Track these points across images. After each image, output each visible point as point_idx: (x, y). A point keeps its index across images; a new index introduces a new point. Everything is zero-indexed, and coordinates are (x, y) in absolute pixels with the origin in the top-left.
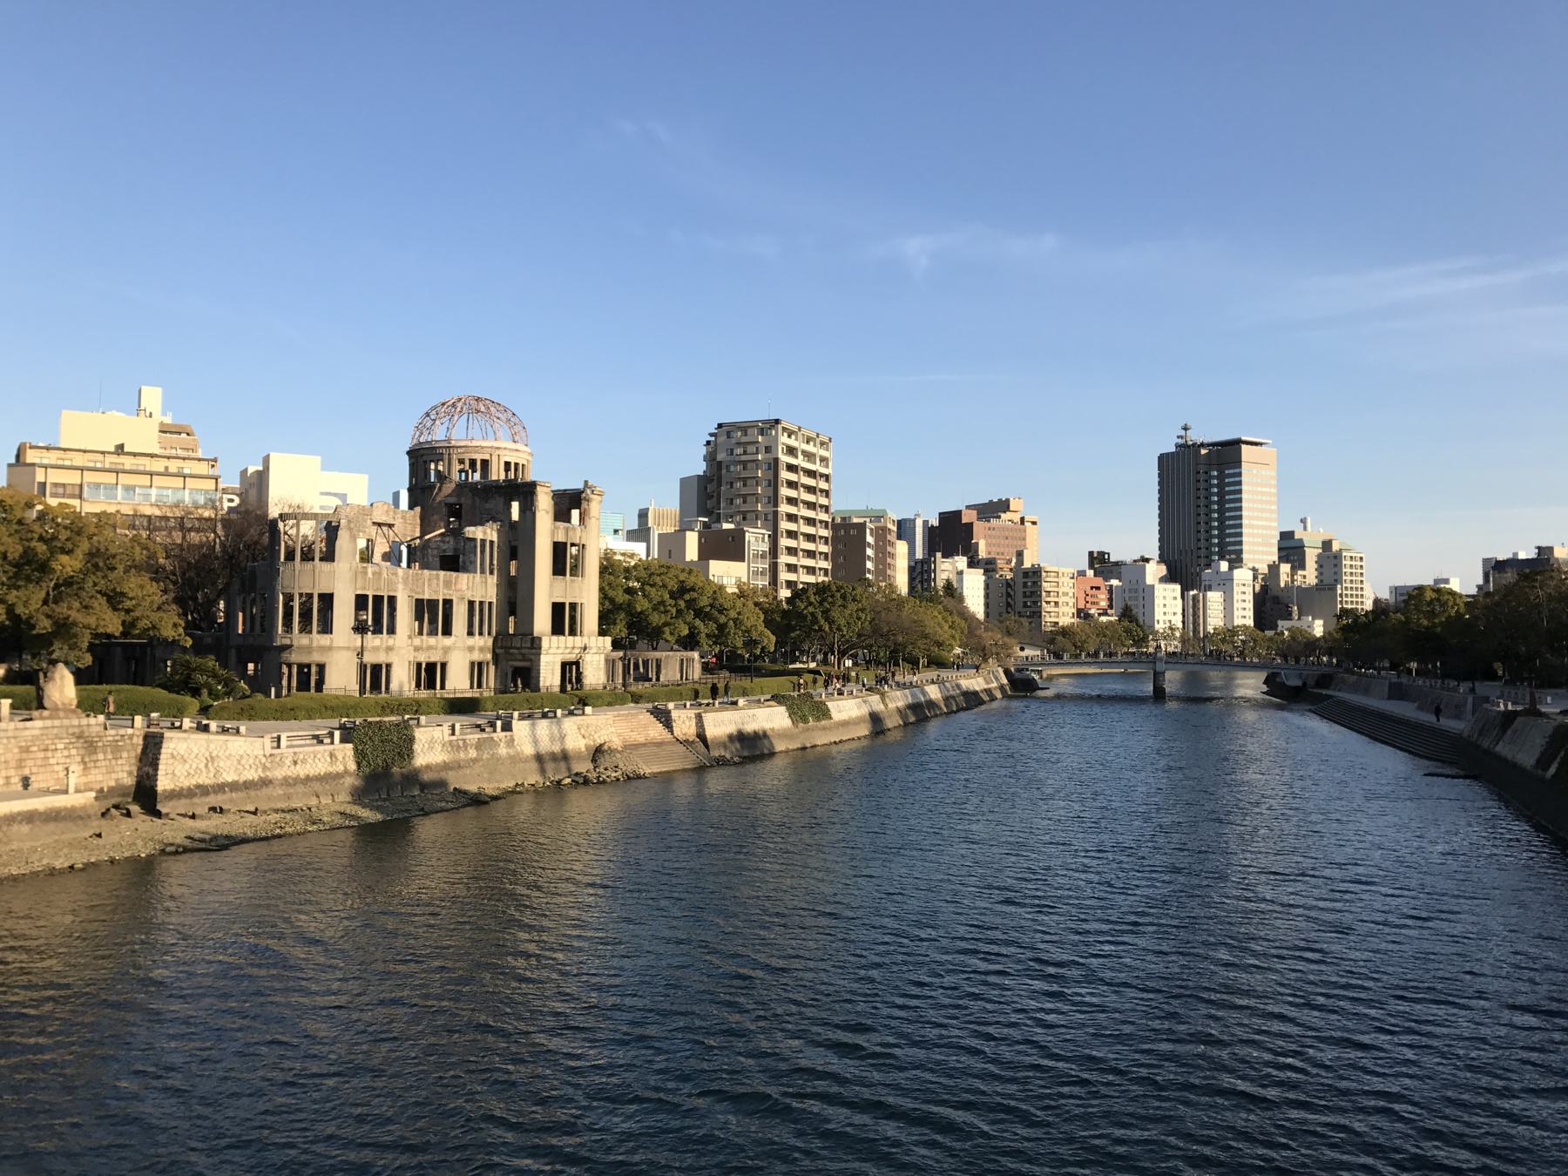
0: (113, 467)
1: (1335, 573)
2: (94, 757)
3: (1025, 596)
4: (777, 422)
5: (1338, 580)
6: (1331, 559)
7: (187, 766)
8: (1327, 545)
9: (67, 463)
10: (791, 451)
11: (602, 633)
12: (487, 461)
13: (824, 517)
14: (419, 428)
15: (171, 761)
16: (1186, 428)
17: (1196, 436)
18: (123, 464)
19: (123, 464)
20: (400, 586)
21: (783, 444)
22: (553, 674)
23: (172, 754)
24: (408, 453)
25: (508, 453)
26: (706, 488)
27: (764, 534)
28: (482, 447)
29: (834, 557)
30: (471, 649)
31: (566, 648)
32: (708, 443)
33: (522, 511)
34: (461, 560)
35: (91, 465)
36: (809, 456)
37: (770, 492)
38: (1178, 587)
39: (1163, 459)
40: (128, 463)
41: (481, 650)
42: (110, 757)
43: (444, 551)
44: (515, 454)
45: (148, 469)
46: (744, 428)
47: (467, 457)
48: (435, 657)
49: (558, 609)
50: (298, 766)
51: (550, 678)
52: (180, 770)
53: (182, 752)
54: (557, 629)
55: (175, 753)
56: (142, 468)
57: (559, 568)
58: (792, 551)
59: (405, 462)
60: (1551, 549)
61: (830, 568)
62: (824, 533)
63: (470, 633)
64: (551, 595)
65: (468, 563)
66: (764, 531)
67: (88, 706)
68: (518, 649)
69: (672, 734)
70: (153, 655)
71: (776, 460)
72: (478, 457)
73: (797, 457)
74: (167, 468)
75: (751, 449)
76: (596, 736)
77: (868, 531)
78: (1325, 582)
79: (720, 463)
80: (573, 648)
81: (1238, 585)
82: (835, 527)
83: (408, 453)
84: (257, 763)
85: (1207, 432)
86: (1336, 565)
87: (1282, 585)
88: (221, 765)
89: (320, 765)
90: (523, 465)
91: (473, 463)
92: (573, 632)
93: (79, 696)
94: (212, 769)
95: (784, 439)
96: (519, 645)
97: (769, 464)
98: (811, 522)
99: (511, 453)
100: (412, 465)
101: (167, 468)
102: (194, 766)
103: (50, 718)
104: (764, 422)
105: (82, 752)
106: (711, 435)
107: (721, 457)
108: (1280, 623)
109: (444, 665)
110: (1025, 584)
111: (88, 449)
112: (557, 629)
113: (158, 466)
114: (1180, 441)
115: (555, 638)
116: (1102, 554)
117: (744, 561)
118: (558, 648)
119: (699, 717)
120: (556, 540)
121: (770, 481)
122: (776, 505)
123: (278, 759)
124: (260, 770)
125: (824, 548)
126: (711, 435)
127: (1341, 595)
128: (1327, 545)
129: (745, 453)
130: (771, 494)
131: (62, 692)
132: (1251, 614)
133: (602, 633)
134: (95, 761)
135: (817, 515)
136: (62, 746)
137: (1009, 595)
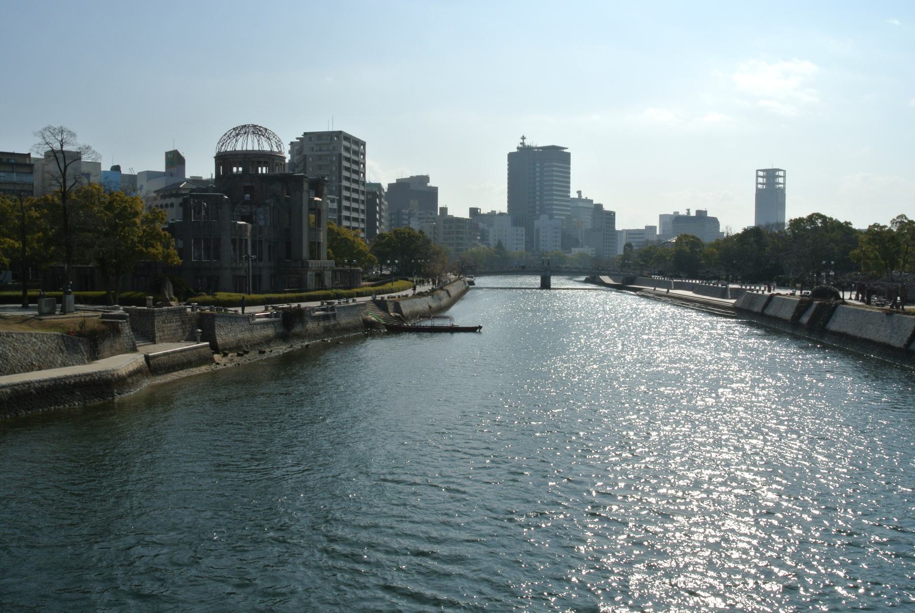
3: (444, 234)
10: (347, 149)
11: (329, 258)
13: (362, 188)
14: (222, 142)
16: (523, 138)
17: (528, 143)
36: (356, 153)
38: (524, 229)
39: (511, 156)
46: (320, 135)
62: (362, 198)
63: (270, 260)
66: (334, 197)
71: (340, 155)
72: (262, 160)
79: (305, 156)
82: (368, 193)
85: (538, 140)
98: (356, 191)
106: (297, 139)
107: (306, 152)
108: (573, 249)
110: (445, 228)
114: (520, 146)
116: (477, 209)
122: (340, 181)
129: (320, 150)
132: (559, 244)
137: (435, 232)
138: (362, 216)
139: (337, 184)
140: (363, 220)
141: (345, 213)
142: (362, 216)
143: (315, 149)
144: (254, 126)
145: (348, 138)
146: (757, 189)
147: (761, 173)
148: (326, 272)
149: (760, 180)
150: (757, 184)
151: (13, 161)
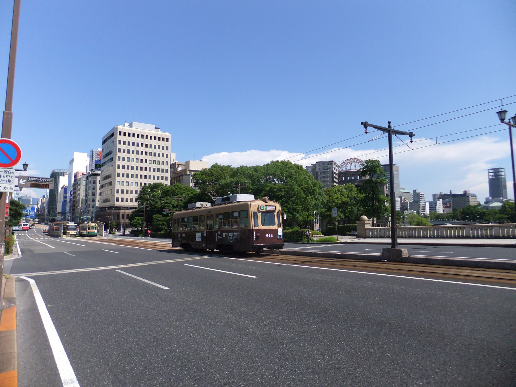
1: (418, 198)
5: (418, 201)
6: (416, 195)
8: (415, 191)
60: (466, 191)
78: (415, 201)
81: (397, 202)
86: (418, 196)
87: (403, 202)
95: (334, 166)
104: (329, 161)
106: (312, 165)
127: (420, 204)
128: (415, 191)
129: (324, 169)
130: (332, 180)
146: (490, 179)
147: (491, 171)
149: (491, 174)
150: (489, 176)
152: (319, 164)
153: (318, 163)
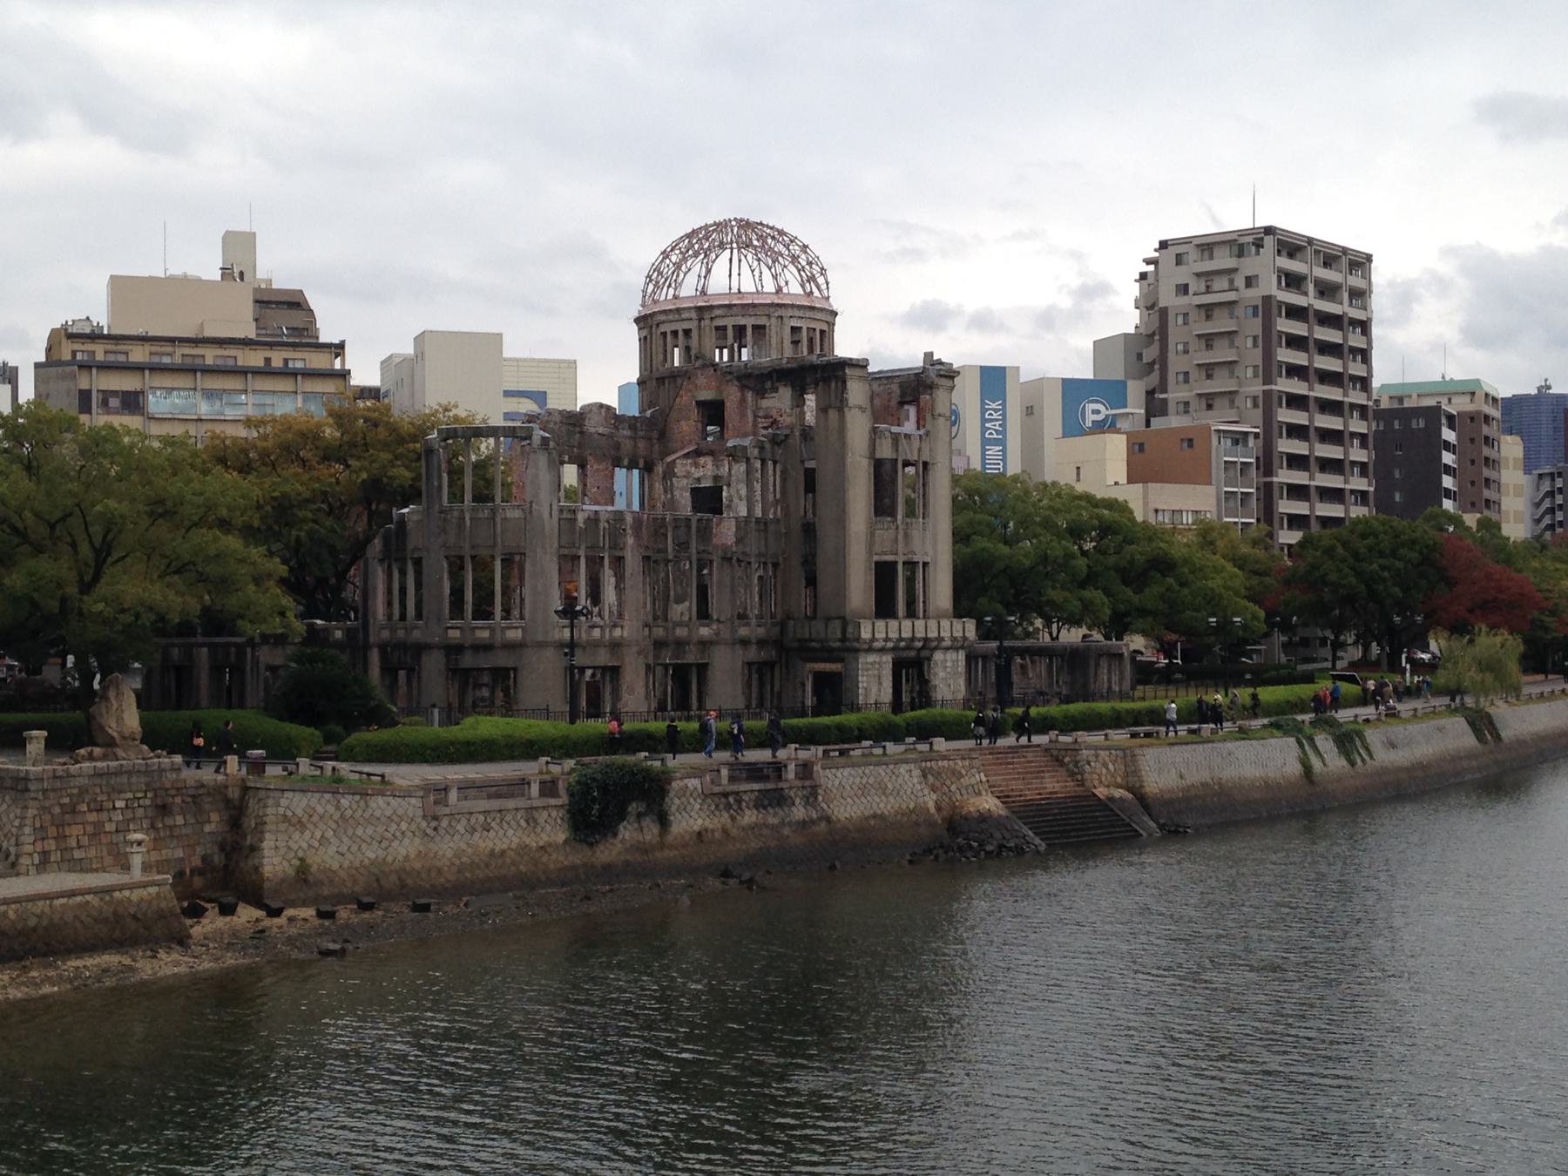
0: (188, 361)
2: (168, 821)
4: (1269, 230)
7: (307, 834)
9: (122, 358)
10: (1293, 281)
11: (959, 612)
12: (763, 327)
13: (1356, 397)
14: (656, 277)
15: (283, 827)
18: (203, 356)
19: (203, 356)
20: (630, 541)
21: (1280, 270)
22: (880, 684)
23: (285, 816)
24: (637, 321)
25: (797, 313)
26: (1140, 356)
27: (1246, 434)
28: (754, 306)
29: (1379, 470)
30: (745, 642)
31: (901, 639)
32: (1143, 276)
33: (823, 410)
34: (724, 494)
35: (156, 359)
36: (1327, 290)
37: (1256, 356)
40: (210, 356)
41: (761, 643)
42: (193, 821)
43: (698, 480)
44: (808, 314)
45: (240, 363)
46: (1207, 246)
47: (729, 322)
48: (691, 657)
49: (884, 574)
50: (477, 835)
51: (874, 690)
52: (300, 841)
53: (299, 812)
54: (884, 609)
55: (289, 814)
56: (231, 362)
57: (883, 504)
58: (1296, 462)
59: (632, 335)
61: (1372, 489)
62: (1358, 426)
64: (870, 553)
65: (736, 500)
67: (153, 738)
68: (821, 641)
69: (1082, 783)
70: (256, 661)
71: (1267, 300)
72: (749, 322)
73: (1306, 294)
74: (268, 360)
75: (1221, 283)
76: (953, 788)
77: (1444, 421)
79: (1164, 312)
80: (913, 639)
82: (1381, 415)
83: (637, 321)
84: (413, 827)
88: (359, 832)
89: (510, 833)
90: (822, 332)
91: (740, 331)
92: (911, 614)
93: (143, 723)
94: (345, 839)
96: (822, 636)
97: (1255, 308)
99: (801, 314)
100: (644, 341)
101: (268, 360)
102: (318, 834)
103: (104, 757)
105: (150, 813)
106: (1148, 262)
107: (1168, 298)
109: (703, 668)
111: (154, 332)
112: (884, 609)
113: (255, 359)
115: (880, 624)
117: (1210, 484)
118: (887, 639)
119: (1129, 758)
120: (878, 456)
121: (1255, 338)
123: (445, 823)
124: (417, 841)
125: (1359, 454)
126: (1148, 262)
129: (1208, 290)
131: (120, 720)
133: (959, 612)
134: (171, 828)
135: (1346, 395)
136: (120, 804)
138: (1359, 483)
139: (1258, 388)
140: (1362, 497)
141: (1285, 476)
142: (1359, 483)
143: (1191, 292)
144: (745, 225)
145: (1291, 246)
148: (938, 656)
151: (299, 365)
152: (1178, 256)
153: (1173, 251)
